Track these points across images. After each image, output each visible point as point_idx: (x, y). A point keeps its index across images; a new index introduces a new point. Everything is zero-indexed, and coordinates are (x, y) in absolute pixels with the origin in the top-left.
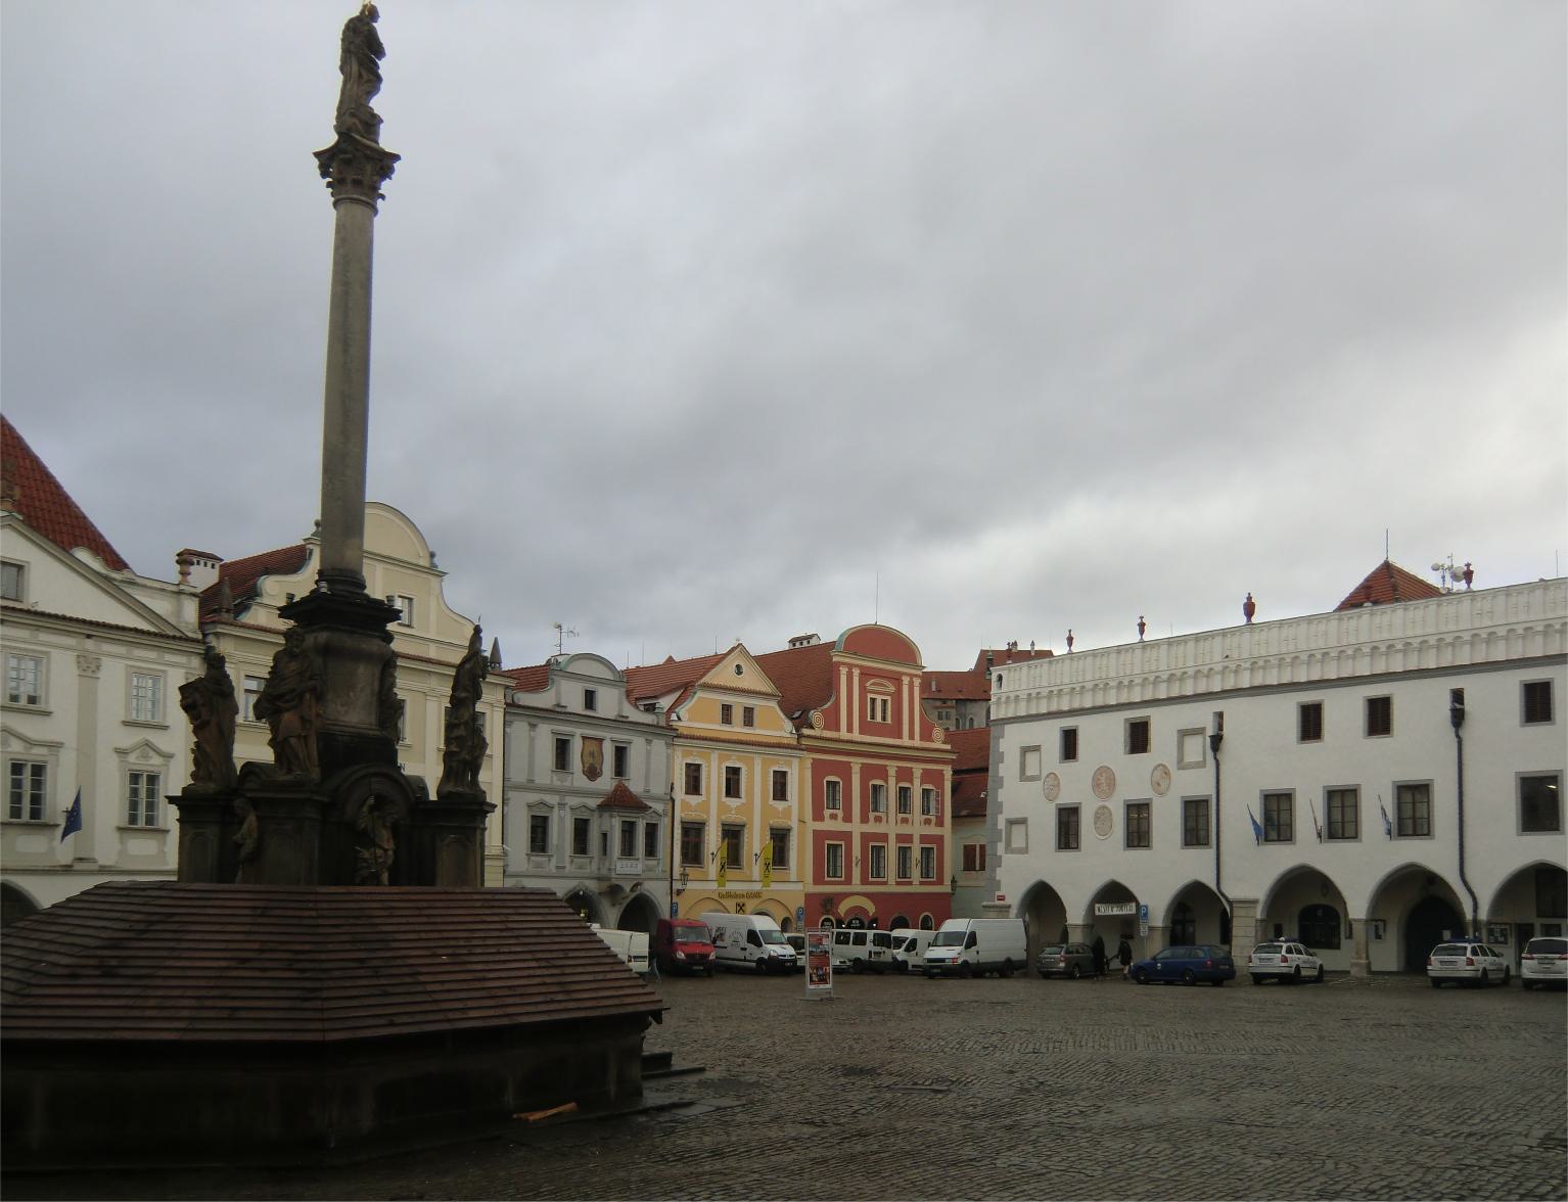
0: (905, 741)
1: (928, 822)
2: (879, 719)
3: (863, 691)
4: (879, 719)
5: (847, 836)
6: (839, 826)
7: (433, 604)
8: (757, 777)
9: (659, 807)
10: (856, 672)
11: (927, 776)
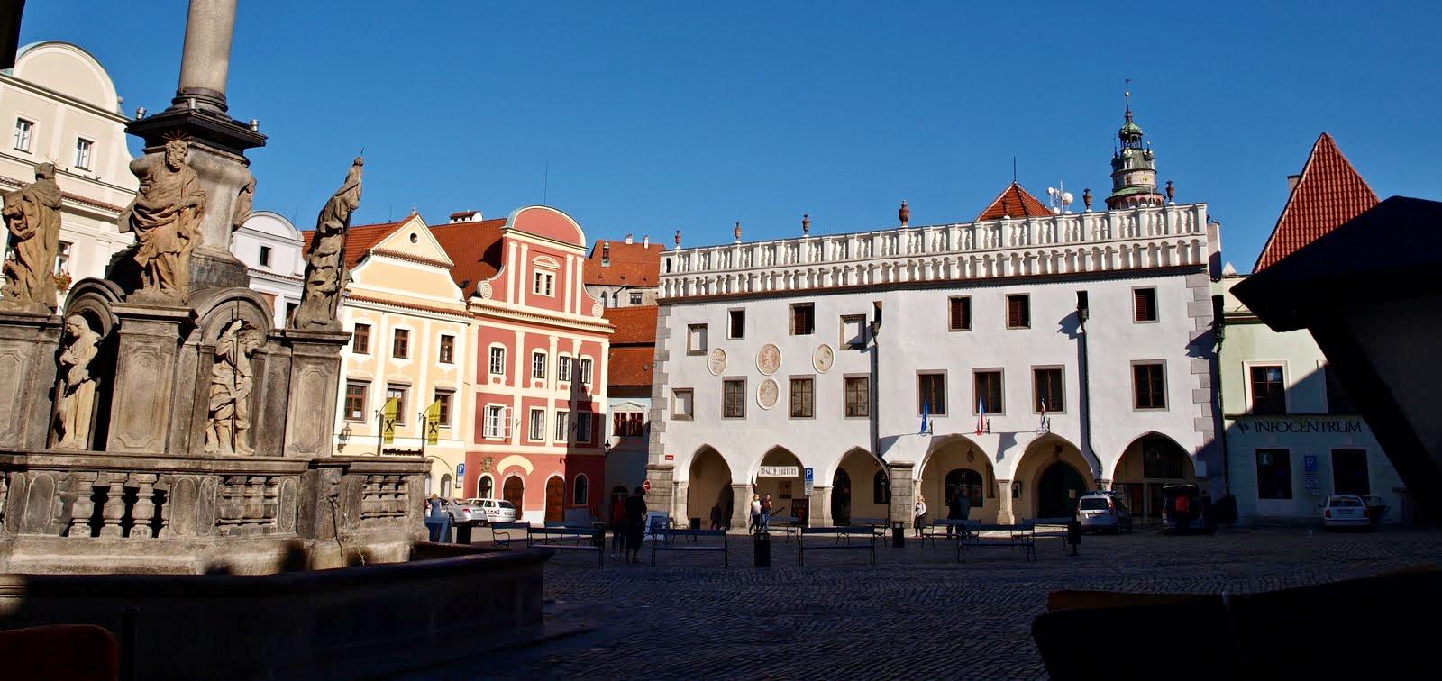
0: (567, 314)
3: (530, 265)
5: (509, 400)
6: (501, 389)
8: (424, 338)
10: (525, 248)
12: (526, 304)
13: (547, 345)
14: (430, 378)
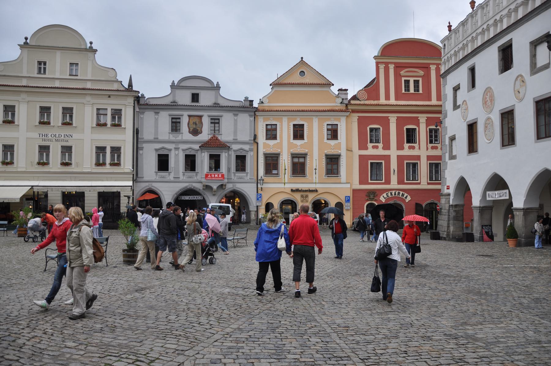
2: (412, 90)
3: (398, 77)
4: (412, 90)
6: (380, 152)
7: (90, 64)
8: (315, 130)
9: (247, 147)
10: (392, 67)
12: (396, 99)
13: (416, 121)
14: (320, 149)
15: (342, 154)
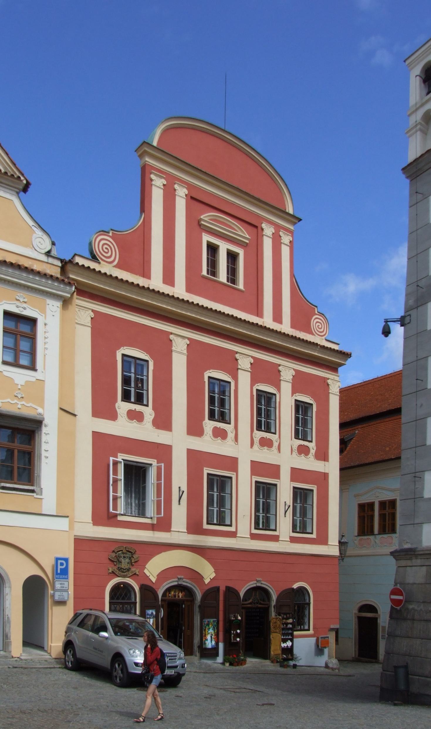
1: (303, 451)
11: (300, 383)
15: (45, 422)
